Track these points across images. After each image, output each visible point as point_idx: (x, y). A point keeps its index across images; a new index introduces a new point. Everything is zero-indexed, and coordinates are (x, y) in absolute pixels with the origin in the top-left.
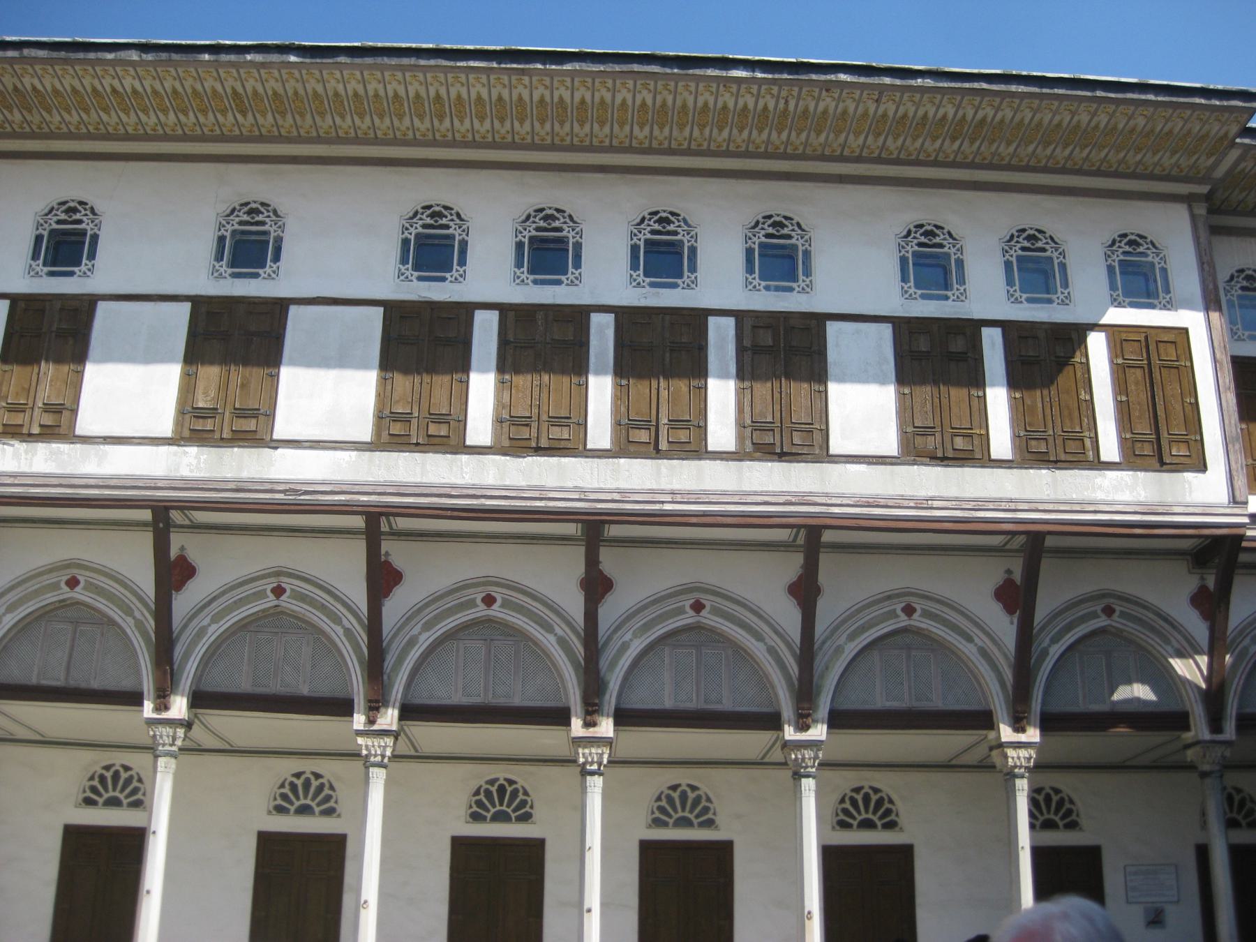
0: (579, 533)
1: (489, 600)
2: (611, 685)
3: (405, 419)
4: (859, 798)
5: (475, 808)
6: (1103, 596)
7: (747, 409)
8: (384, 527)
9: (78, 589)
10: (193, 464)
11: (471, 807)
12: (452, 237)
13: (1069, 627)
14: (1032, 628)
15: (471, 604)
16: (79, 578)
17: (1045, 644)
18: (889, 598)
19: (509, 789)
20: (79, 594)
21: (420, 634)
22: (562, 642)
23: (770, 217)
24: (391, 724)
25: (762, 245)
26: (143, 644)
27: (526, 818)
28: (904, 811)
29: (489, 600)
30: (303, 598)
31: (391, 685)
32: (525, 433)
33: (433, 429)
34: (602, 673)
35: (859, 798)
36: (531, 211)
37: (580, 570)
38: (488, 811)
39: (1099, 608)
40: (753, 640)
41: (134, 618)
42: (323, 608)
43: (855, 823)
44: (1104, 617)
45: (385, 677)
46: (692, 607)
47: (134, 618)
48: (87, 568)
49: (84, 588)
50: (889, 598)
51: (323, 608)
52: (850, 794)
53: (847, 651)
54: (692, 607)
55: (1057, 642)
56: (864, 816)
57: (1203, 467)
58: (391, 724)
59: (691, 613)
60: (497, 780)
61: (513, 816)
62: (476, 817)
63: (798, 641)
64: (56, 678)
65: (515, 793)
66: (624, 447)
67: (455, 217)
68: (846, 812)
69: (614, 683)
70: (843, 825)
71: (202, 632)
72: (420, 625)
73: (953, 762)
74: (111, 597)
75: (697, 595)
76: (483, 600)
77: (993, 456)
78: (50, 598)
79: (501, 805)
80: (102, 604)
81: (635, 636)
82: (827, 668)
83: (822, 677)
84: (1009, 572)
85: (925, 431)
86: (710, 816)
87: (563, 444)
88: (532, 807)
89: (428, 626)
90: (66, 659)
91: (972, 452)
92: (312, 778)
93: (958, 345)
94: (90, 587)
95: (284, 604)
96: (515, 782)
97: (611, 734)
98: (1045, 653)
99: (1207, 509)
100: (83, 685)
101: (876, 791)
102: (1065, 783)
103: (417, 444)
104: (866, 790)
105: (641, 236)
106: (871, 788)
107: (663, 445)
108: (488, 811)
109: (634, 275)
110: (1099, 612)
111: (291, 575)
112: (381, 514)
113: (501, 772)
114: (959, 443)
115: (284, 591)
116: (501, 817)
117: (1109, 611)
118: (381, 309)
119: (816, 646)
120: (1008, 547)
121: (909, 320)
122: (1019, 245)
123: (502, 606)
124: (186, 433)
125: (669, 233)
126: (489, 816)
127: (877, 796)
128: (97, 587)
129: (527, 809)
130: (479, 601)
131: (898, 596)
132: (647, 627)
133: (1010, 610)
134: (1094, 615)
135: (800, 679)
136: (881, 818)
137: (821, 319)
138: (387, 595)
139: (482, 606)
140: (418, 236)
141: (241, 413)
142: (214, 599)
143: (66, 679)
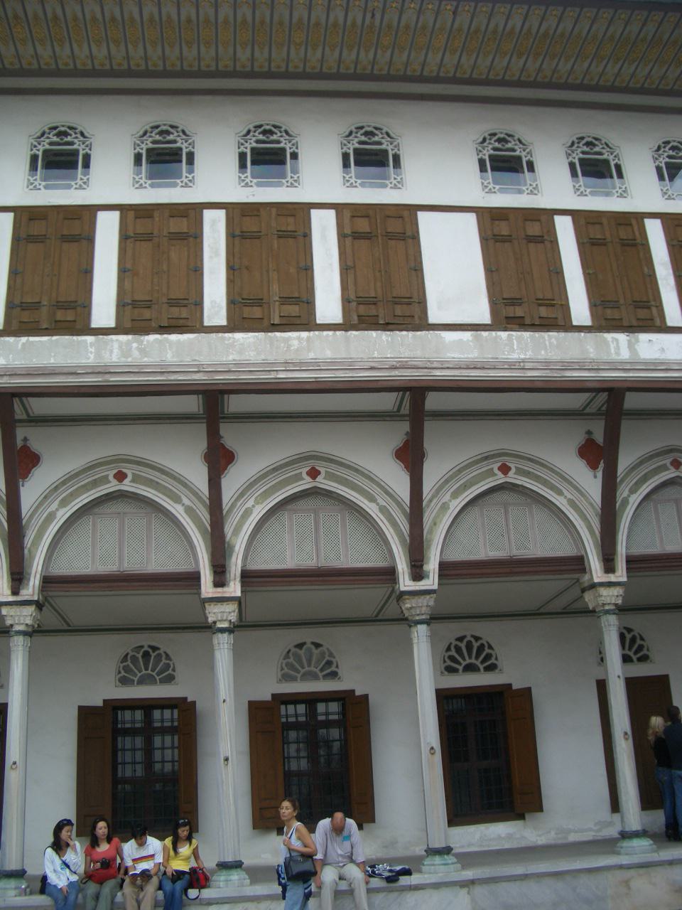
0: (201, 412)
1: (121, 476)
2: (237, 548)
4: (463, 645)
7: (351, 286)
8: (19, 413)
11: (120, 672)
12: (77, 151)
13: (644, 479)
14: (616, 477)
15: (105, 480)
17: (625, 494)
18: (486, 458)
19: (153, 655)
21: (57, 510)
22: (189, 511)
23: (362, 128)
24: (33, 595)
25: (356, 150)
27: (170, 679)
28: (501, 653)
31: (32, 558)
32: (147, 314)
33: (60, 315)
34: (228, 539)
35: (463, 645)
36: (148, 127)
37: (203, 445)
39: (668, 462)
40: (366, 502)
43: (461, 668)
44: (673, 469)
45: (26, 551)
46: (309, 473)
50: (486, 458)
52: (454, 643)
53: (452, 507)
55: (636, 492)
56: (468, 661)
58: (33, 595)
59: (308, 479)
60: (142, 647)
61: (158, 678)
62: (124, 681)
63: (408, 504)
66: (239, 321)
67: (79, 135)
68: (452, 658)
69: (239, 544)
70: (450, 670)
73: (542, 610)
75: (312, 463)
76: (115, 476)
77: (575, 323)
79: (146, 669)
81: (257, 502)
82: (435, 524)
83: (431, 532)
84: (589, 433)
85: (513, 302)
86: (333, 668)
87: (181, 322)
88: (174, 670)
89: (64, 503)
91: (553, 317)
96: (158, 649)
97: (238, 594)
98: (625, 502)
101: (477, 639)
102: (639, 623)
103: (46, 329)
104: (469, 638)
105: (247, 145)
106: (472, 636)
109: (243, 177)
110: (668, 465)
112: (14, 395)
113: (145, 640)
114: (543, 312)
118: (12, 215)
119: (424, 503)
120: (588, 410)
122: (580, 150)
123: (133, 481)
126: (136, 679)
127: (478, 644)
129: (170, 671)
130: (111, 478)
131: (493, 456)
133: (593, 466)
134: (663, 468)
135: (411, 535)
136: (482, 662)
137: (411, 211)
138: (26, 474)
139: (115, 482)
140: (45, 152)
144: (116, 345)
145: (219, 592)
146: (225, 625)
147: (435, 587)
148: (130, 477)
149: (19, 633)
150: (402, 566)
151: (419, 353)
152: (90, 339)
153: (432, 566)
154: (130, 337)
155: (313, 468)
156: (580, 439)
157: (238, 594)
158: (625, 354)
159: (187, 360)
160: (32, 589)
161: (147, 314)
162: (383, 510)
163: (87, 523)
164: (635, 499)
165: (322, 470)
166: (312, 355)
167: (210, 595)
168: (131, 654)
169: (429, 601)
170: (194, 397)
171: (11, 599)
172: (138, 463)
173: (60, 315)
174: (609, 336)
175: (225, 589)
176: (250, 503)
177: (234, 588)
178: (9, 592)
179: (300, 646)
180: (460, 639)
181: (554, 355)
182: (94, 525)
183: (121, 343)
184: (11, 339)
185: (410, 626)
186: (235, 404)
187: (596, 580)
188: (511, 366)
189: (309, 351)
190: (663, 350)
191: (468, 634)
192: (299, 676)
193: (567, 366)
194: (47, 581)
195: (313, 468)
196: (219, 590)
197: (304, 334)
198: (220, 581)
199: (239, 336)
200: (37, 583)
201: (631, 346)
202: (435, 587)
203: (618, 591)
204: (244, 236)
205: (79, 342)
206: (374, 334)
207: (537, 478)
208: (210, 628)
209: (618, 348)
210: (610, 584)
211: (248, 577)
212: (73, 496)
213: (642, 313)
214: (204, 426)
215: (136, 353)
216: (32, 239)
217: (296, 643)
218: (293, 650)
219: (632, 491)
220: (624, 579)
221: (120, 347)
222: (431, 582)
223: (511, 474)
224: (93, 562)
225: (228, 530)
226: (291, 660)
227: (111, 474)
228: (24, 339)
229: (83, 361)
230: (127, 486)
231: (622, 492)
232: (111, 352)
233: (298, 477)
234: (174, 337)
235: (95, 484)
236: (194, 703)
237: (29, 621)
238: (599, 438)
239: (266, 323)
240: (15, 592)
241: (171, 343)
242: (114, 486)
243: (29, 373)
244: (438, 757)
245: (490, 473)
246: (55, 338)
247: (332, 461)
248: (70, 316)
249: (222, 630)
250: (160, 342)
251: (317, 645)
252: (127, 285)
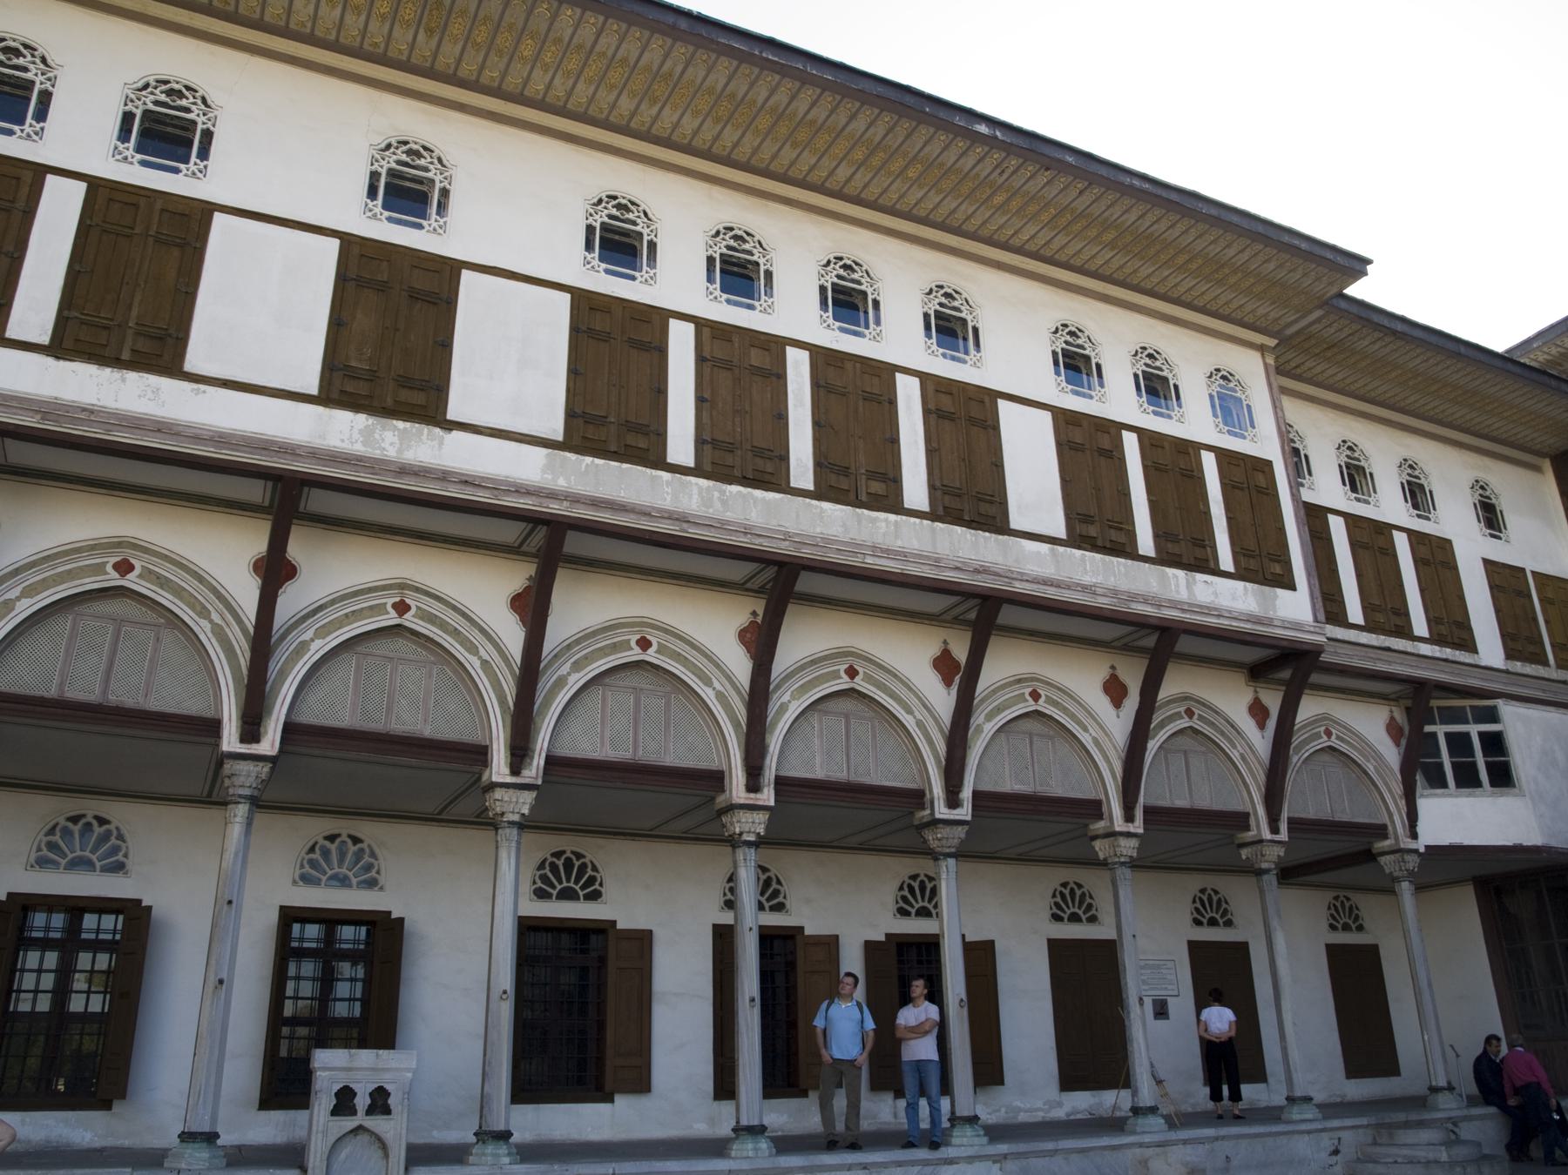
2: (771, 749)
3: (601, 421)
4: (916, 885)
5: (539, 884)
6: (1186, 698)
7: (936, 471)
9: (131, 576)
10: (344, 432)
15: (625, 645)
16: (133, 561)
18: (1019, 681)
20: (132, 581)
26: (222, 656)
27: (594, 896)
29: (644, 644)
30: (431, 619)
32: (729, 460)
33: (631, 439)
35: (916, 885)
38: (554, 887)
39: (1182, 709)
41: (211, 621)
42: (455, 633)
43: (913, 911)
47: (211, 621)
48: (146, 550)
49: (140, 576)
51: (455, 633)
54: (847, 672)
57: (1291, 587)
61: (581, 894)
64: (86, 689)
65: (583, 868)
69: (774, 742)
71: (303, 647)
72: (568, 665)
74: (178, 591)
76: (638, 642)
78: (90, 583)
80: (165, 598)
81: (793, 697)
85: (1087, 519)
86: (781, 899)
87: (767, 478)
90: (103, 667)
92: (327, 843)
93: (1105, 442)
94: (148, 574)
95: (407, 624)
99: (1297, 626)
100: (129, 701)
104: (922, 877)
107: (864, 498)
108: (554, 887)
111: (417, 590)
114: (1114, 535)
115: (408, 608)
116: (567, 895)
117: (1190, 713)
121: (1064, 411)
123: (658, 652)
124: (335, 395)
125: (853, 281)
128: (159, 576)
129: (597, 886)
130: (633, 644)
131: (1026, 680)
132: (804, 689)
139: (637, 650)
141: (405, 382)
142: (321, 608)
143: (104, 692)
144: (695, 491)
145: (751, 799)
146: (752, 838)
147: (969, 818)
148: (655, 647)
149: (512, 823)
150: (938, 790)
151: (1000, 560)
152: (666, 476)
153: (966, 794)
154: (711, 483)
155: (851, 667)
156: (934, 650)
157: (772, 803)
158: (1183, 595)
159: (773, 524)
160: (534, 770)
161: (729, 460)
162: (920, 724)
163: (597, 693)
164: (990, 728)
165: (654, 641)
166: (899, 543)
167: (742, 801)
168: (550, 859)
169: (961, 832)
170: (261, 483)
171: (509, 779)
172: (666, 631)
173: (631, 439)
174: (1170, 571)
175: (758, 796)
176: (786, 698)
177: (767, 797)
178: (507, 771)
179: (332, 838)
180: (557, 855)
181: (1124, 585)
182: (604, 700)
183: (700, 489)
184: (572, 456)
185: (936, 859)
186: (318, 501)
187: (938, 816)
188: (1085, 588)
189: (897, 537)
190: (1216, 594)
191: (568, 849)
192: (324, 878)
193: (1133, 597)
194: (551, 761)
195: (851, 667)
196: (752, 795)
197: (892, 517)
198: (753, 786)
199: (826, 505)
200: (542, 763)
201: (1189, 586)
202: (969, 818)
203: (1134, 843)
204: (591, 333)
205: (653, 478)
206: (958, 529)
207: (1065, 710)
208: (734, 842)
209: (1177, 586)
210: (1129, 835)
211: (781, 783)
212: (44, 584)
213: (1199, 552)
214: (1146, 662)
215: (718, 505)
216: (361, 283)
217: (327, 833)
218: (322, 842)
219: (989, 717)
220: (1141, 831)
221: (700, 493)
222: (965, 812)
223: (1041, 701)
224: (603, 743)
225: (274, 667)
226: (316, 856)
227: (634, 638)
228: (589, 459)
229: (659, 503)
230: (651, 656)
231: (978, 719)
232: (690, 496)
233: (835, 675)
234: (758, 493)
235: (615, 648)
236: (401, 920)
237: (526, 811)
238: (961, 653)
239: (737, 473)
240: (515, 771)
241: (755, 500)
242: (635, 654)
243: (596, 503)
244: (757, 1011)
245: (1021, 698)
246: (625, 466)
247: (1204, 705)
248: (642, 443)
249: (749, 844)
250: (743, 496)
251: (356, 840)
252: (706, 419)
